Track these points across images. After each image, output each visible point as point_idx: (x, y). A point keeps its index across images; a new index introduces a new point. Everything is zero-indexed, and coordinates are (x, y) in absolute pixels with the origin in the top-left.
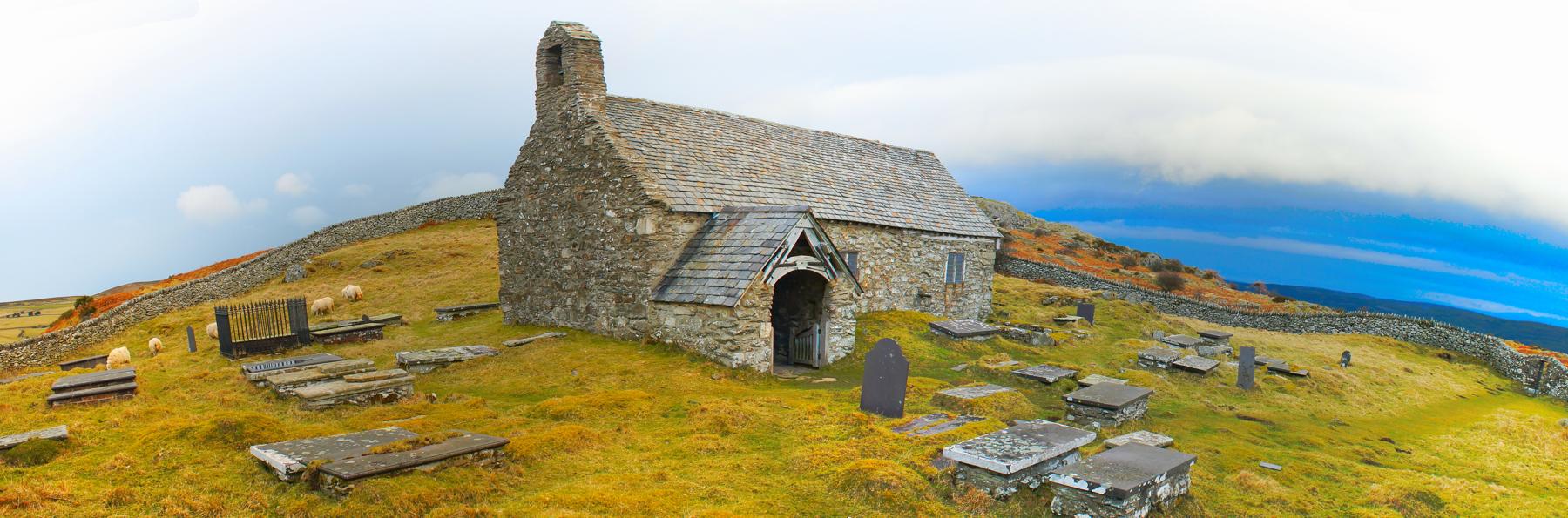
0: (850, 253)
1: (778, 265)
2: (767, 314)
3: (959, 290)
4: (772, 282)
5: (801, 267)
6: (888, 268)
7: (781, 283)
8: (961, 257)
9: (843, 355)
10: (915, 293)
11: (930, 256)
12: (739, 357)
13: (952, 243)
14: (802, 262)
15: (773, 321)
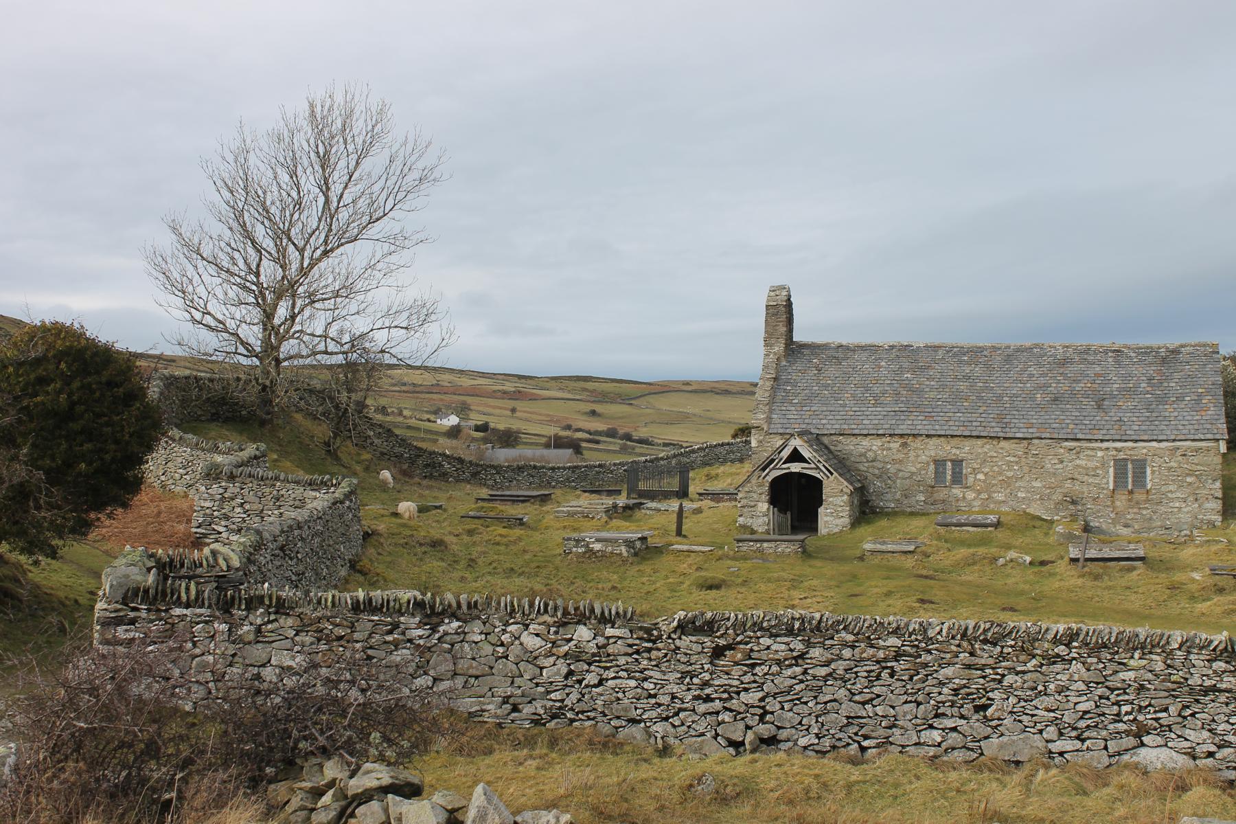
0: (951, 461)
1: (774, 468)
2: (765, 497)
3: (1139, 496)
4: (769, 479)
5: (793, 470)
6: (1010, 474)
7: (775, 482)
8: (1140, 466)
9: (837, 530)
10: (1057, 497)
11: (1078, 462)
12: (741, 520)
13: (1116, 449)
14: (796, 467)
15: (773, 501)
